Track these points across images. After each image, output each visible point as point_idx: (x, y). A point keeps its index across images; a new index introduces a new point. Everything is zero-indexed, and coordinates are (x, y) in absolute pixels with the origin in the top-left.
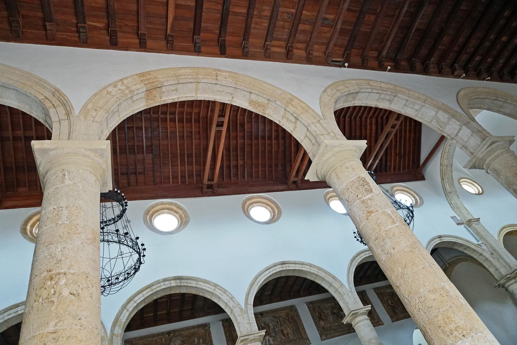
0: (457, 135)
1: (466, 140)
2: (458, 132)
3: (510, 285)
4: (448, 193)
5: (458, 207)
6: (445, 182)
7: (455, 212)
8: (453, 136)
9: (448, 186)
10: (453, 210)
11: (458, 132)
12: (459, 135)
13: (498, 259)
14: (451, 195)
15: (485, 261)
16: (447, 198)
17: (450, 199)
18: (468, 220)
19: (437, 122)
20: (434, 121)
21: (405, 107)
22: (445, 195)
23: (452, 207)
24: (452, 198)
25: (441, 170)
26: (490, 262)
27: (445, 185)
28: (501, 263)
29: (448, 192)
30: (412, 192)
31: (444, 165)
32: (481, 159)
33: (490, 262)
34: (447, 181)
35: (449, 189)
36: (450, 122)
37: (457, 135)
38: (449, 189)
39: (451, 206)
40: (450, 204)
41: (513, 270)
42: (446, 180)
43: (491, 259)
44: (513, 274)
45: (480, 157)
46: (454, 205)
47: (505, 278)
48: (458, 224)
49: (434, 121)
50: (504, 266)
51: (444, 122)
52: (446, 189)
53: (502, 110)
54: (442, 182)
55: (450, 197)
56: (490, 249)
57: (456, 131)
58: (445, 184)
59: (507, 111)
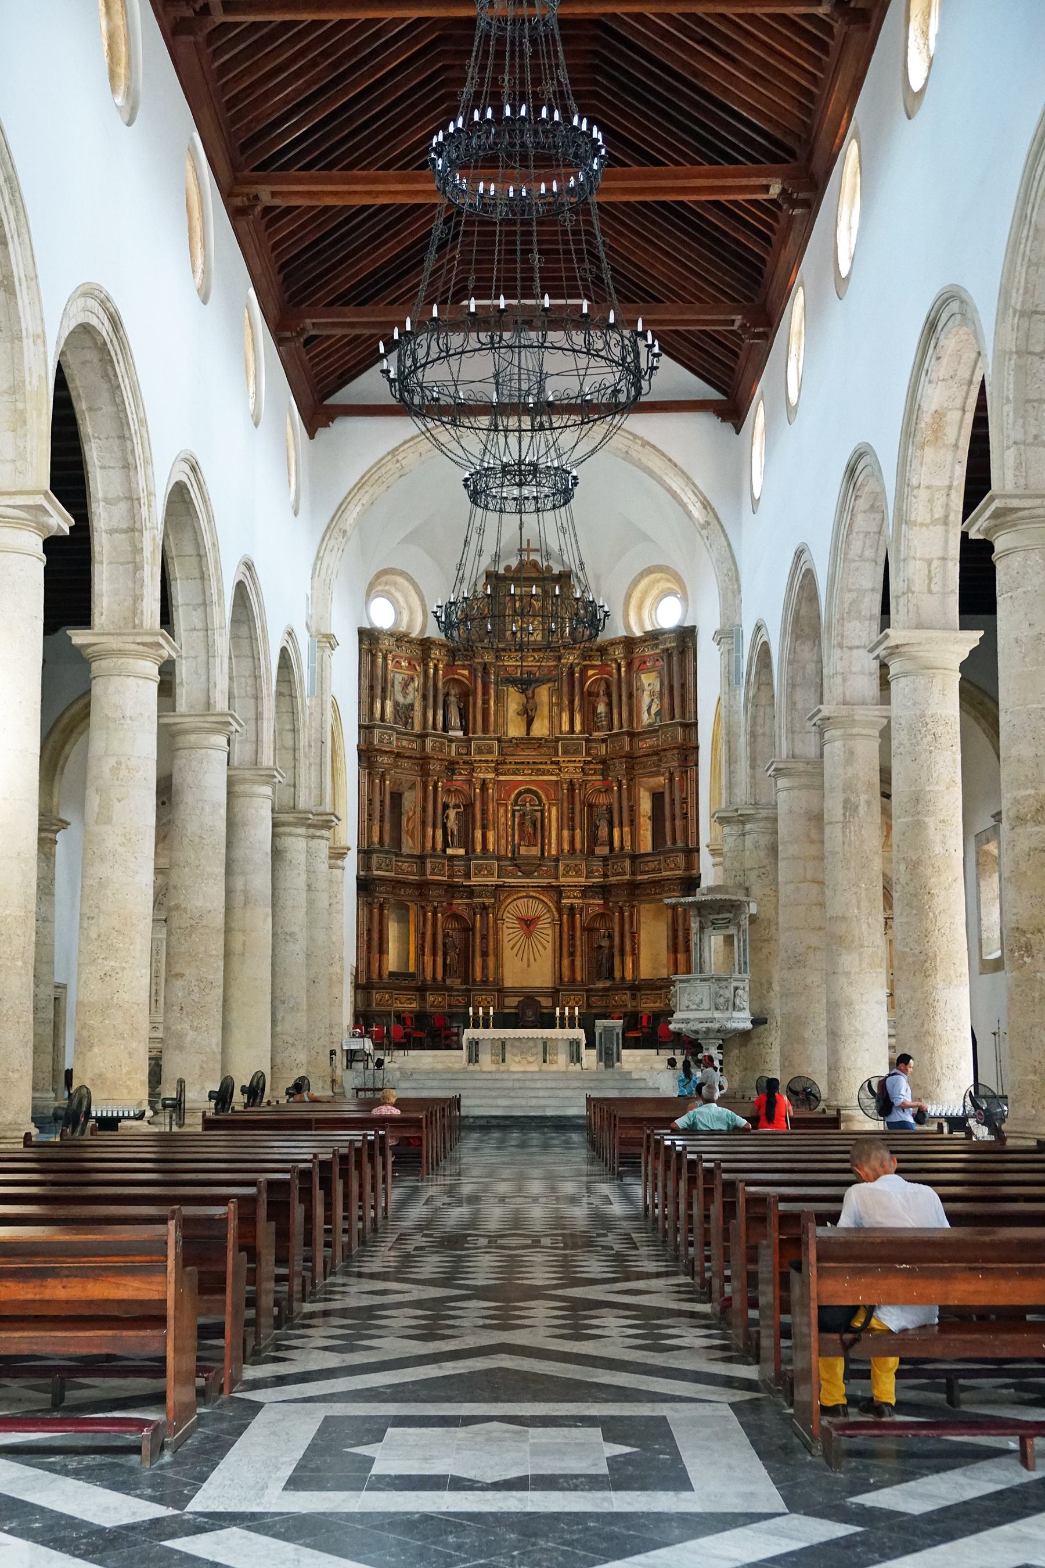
0: (850, 648)
1: (854, 670)
2: (858, 647)
3: (290, 835)
4: (337, 529)
5: (328, 581)
6: (357, 497)
7: (312, 588)
8: (845, 644)
9: (354, 515)
10: (312, 577)
11: (858, 647)
12: (855, 651)
13: (310, 764)
14: (340, 539)
15: (285, 748)
16: (323, 539)
17: (330, 546)
18: (323, 632)
19: (854, 601)
20: (854, 595)
21: (861, 536)
22: (328, 527)
23: (314, 569)
24: (336, 549)
25: (379, 464)
26: (295, 758)
27: (352, 505)
28: (310, 779)
29: (341, 525)
30: (292, 454)
31: (398, 461)
32: (854, 720)
33: (295, 758)
34: (363, 501)
35: (348, 523)
36: (867, 623)
37: (850, 648)
38: (351, 521)
39: (315, 564)
40: (317, 558)
41: (321, 809)
42: (367, 497)
43: (301, 755)
44: (316, 818)
45: (857, 718)
46: (324, 567)
47: (301, 816)
48: (307, 624)
49: (854, 595)
50: (310, 788)
51: (860, 612)
52: (348, 512)
53: (803, 604)
54: (353, 489)
55: (333, 542)
56: (313, 730)
57: (856, 643)
58: (354, 502)
59: (803, 612)
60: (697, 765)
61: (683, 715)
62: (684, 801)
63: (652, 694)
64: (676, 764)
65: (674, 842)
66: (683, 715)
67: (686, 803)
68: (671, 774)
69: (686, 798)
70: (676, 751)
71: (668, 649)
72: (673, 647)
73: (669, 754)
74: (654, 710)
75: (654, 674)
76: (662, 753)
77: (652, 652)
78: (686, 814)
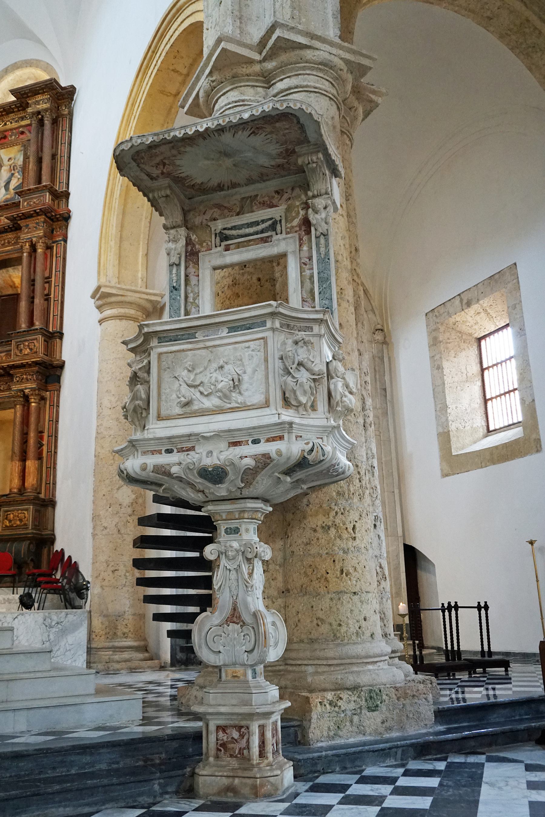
60: (65, 241)
61: (53, 179)
62: (47, 280)
63: (13, 168)
64: (41, 233)
65: (31, 323)
66: (53, 179)
67: (49, 283)
68: (33, 248)
69: (50, 277)
70: (42, 218)
71: (39, 113)
72: (46, 110)
73: (31, 223)
74: (14, 183)
75: (16, 148)
76: (22, 223)
77: (14, 125)
78: (48, 295)
